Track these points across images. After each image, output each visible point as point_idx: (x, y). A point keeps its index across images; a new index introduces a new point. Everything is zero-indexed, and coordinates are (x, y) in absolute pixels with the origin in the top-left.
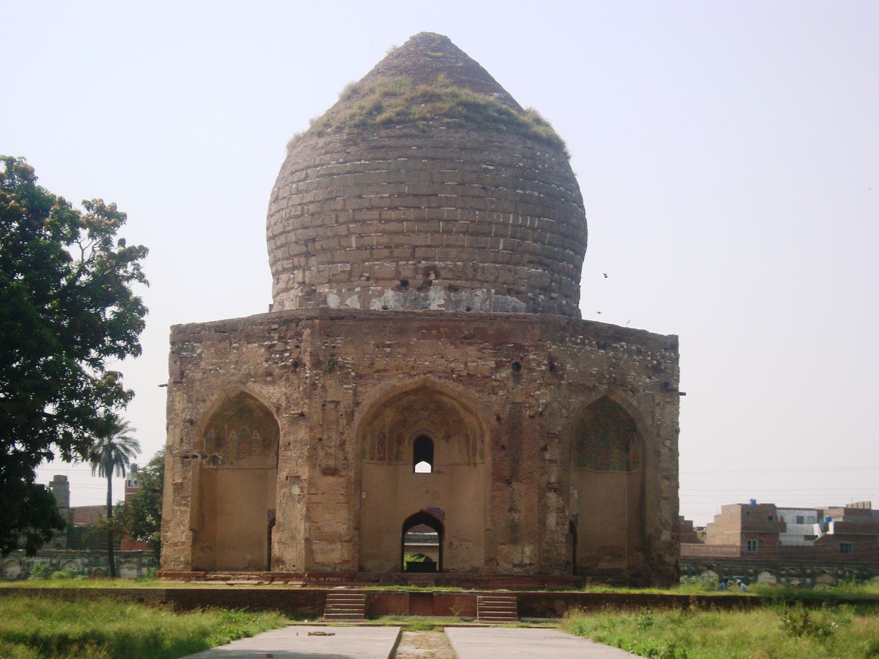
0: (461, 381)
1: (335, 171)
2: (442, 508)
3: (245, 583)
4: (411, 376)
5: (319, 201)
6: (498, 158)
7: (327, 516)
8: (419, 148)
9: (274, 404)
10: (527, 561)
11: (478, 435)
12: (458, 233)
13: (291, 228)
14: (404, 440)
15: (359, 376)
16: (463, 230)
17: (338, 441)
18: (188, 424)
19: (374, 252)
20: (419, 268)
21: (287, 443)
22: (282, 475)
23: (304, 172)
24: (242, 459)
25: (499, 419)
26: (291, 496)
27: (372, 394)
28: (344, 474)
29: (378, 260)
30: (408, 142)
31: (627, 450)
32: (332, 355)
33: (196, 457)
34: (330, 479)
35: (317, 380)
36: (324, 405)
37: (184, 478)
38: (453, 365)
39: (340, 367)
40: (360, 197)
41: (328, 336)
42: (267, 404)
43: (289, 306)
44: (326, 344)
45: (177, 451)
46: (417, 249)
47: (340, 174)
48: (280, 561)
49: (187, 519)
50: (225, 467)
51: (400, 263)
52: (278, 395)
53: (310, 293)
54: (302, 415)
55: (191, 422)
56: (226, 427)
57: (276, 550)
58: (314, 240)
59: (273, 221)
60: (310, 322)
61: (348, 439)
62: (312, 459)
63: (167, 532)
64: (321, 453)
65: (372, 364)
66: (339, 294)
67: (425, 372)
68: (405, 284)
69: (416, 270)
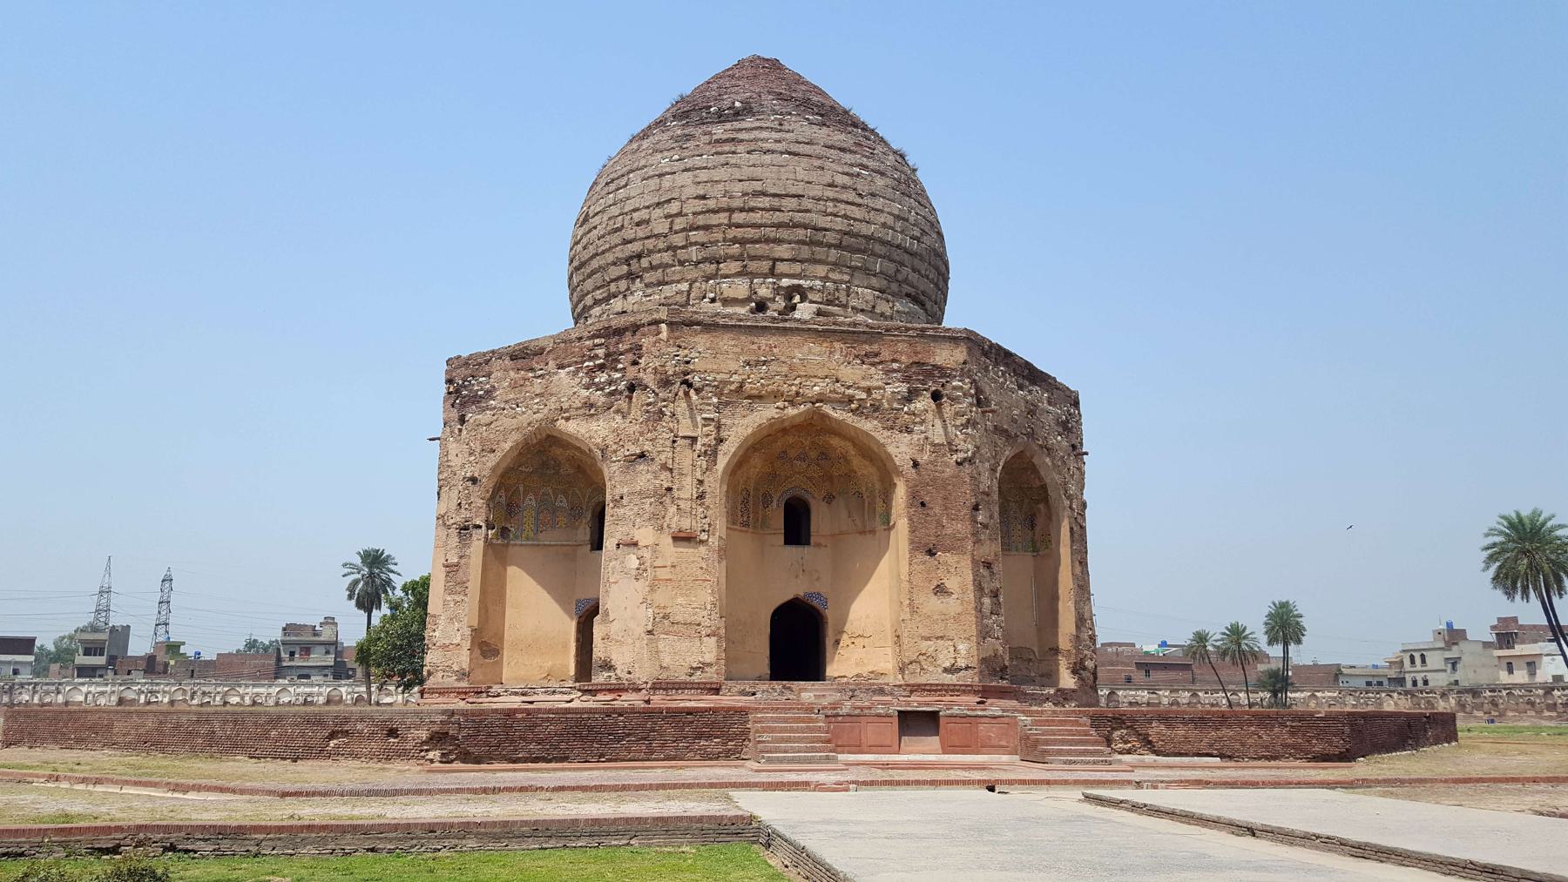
0: (862, 413)
1: (668, 170)
2: (823, 591)
4: (792, 403)
5: (648, 207)
6: (871, 163)
7: (680, 600)
9: (597, 445)
10: (961, 663)
11: (877, 491)
12: (830, 246)
13: (608, 246)
14: (772, 502)
16: (833, 242)
17: (694, 492)
18: (469, 484)
19: (721, 265)
20: (782, 287)
21: (617, 497)
22: (609, 543)
23: (626, 178)
24: (541, 532)
27: (743, 425)
28: (704, 536)
29: (727, 276)
31: (1033, 527)
32: (686, 373)
33: (480, 527)
35: (664, 406)
36: (674, 442)
37: (461, 557)
38: (850, 391)
39: (695, 390)
40: (703, 197)
41: (680, 347)
44: (677, 358)
45: (452, 521)
46: (777, 263)
47: (675, 173)
48: (607, 666)
50: (518, 542)
51: (755, 281)
52: (603, 433)
54: (642, 455)
55: (474, 480)
56: (521, 489)
58: (639, 256)
60: (654, 327)
61: (709, 490)
63: (434, 631)
65: (741, 387)
67: (814, 400)
69: (777, 290)
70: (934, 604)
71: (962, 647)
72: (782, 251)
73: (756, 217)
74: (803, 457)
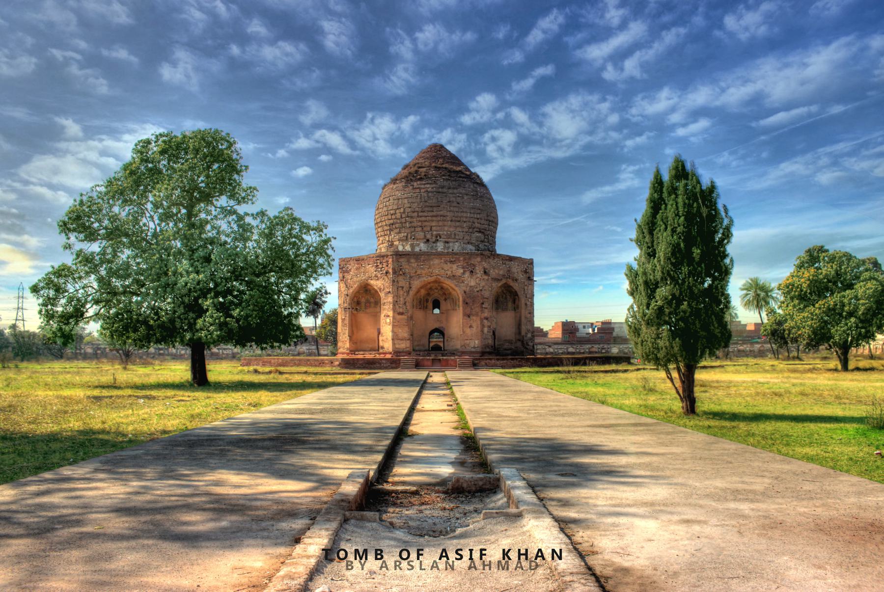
3: (369, 356)
8: (432, 188)
15: (411, 277)
22: (382, 315)
25: (465, 292)
26: (386, 323)
27: (416, 284)
30: (428, 186)
31: (514, 303)
34: (400, 316)
42: (376, 288)
43: (383, 250)
48: (383, 348)
49: (347, 332)
53: (391, 244)
55: (347, 295)
57: (381, 344)
59: (377, 217)
62: (394, 310)
64: (397, 307)
66: (403, 245)
68: (428, 240)
70: (468, 331)
71: (477, 342)
72: (434, 224)
73: (425, 214)
74: (437, 289)
